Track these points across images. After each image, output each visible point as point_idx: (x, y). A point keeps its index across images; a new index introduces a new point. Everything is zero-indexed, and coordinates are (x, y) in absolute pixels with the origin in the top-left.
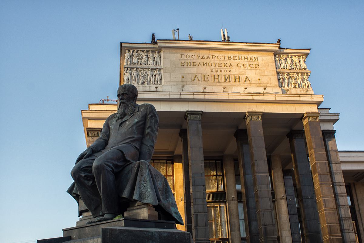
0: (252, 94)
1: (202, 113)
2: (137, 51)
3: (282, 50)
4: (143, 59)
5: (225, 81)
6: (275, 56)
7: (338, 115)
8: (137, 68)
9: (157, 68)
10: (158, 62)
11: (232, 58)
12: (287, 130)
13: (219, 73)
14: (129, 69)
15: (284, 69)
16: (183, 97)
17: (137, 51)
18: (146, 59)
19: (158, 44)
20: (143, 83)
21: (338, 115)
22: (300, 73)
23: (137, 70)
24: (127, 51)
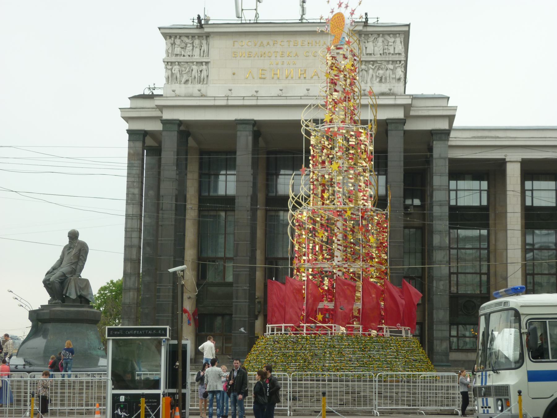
3: (369, 29)
4: (187, 48)
14: (169, 64)
16: (231, 103)
17: (180, 36)
18: (191, 48)
20: (187, 82)
21: (455, 109)
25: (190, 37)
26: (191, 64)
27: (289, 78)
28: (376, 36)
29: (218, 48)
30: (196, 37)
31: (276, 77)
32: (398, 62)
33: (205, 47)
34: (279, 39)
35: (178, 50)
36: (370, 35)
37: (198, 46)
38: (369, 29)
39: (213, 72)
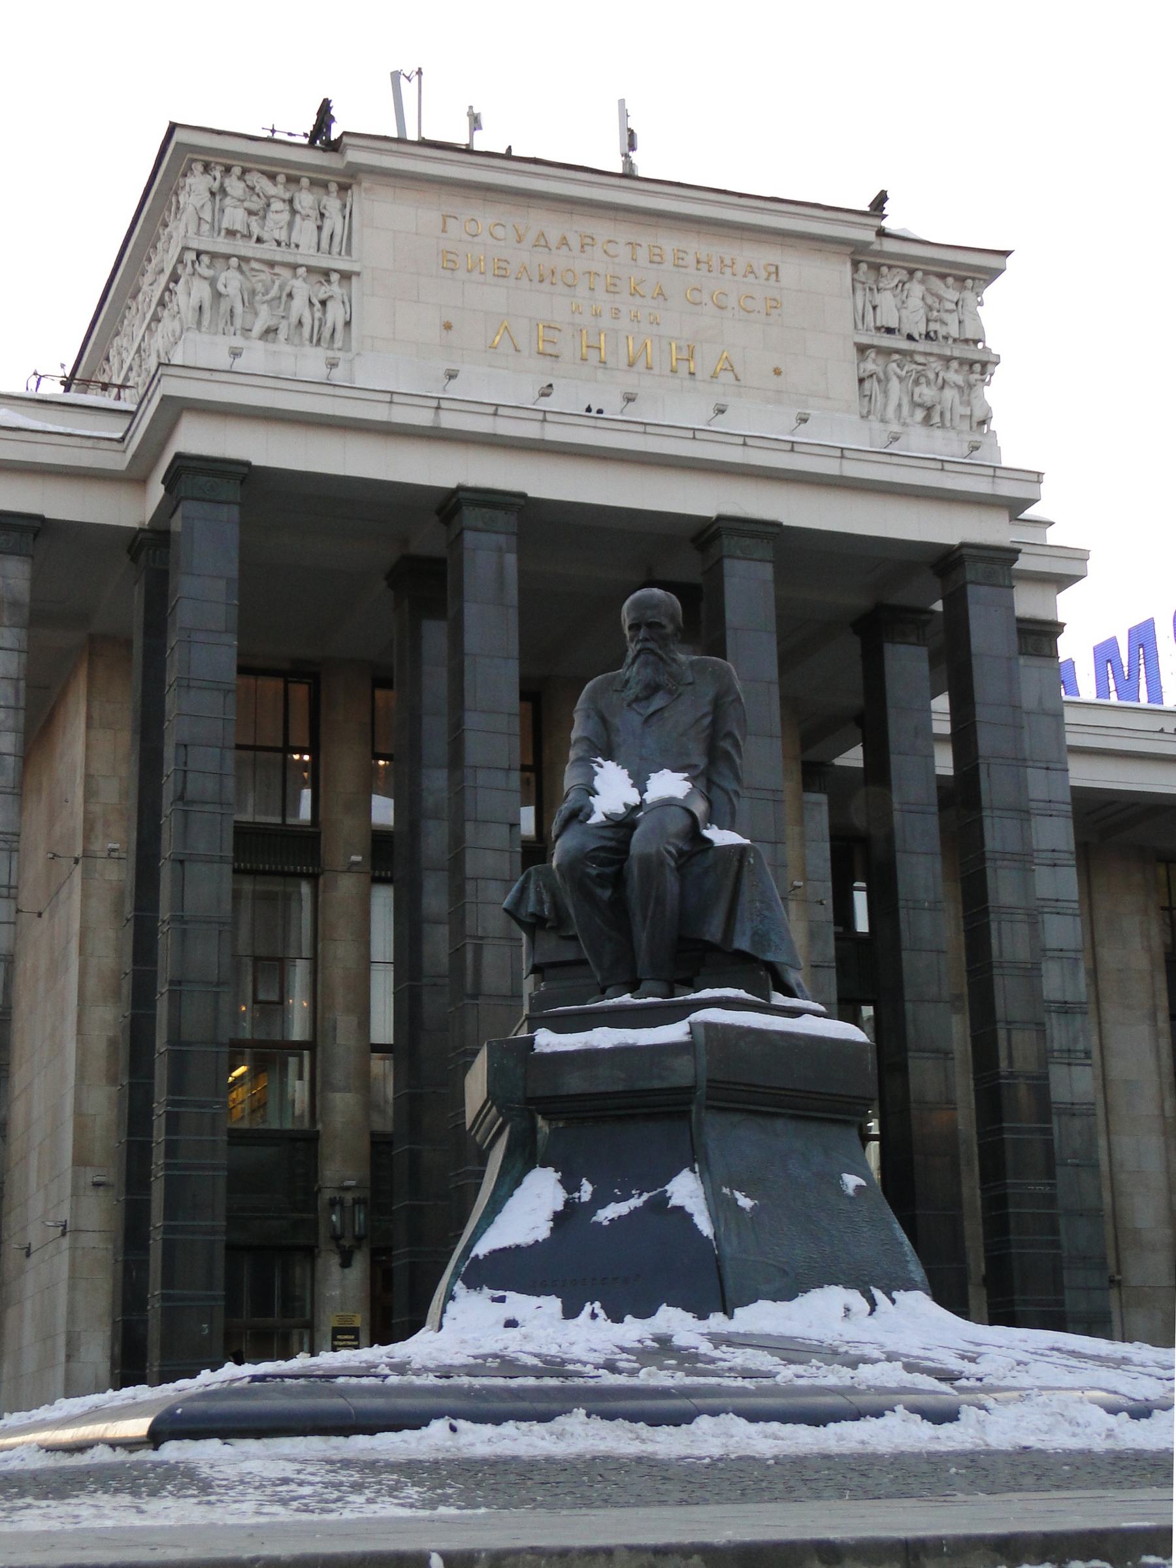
0: (745, 441)
1: (522, 502)
2: (245, 171)
3: (889, 246)
4: (271, 216)
5: (631, 365)
6: (855, 265)
7: (1081, 556)
8: (243, 259)
9: (335, 271)
10: (337, 239)
11: (669, 257)
12: (861, 602)
13: (606, 322)
14: (205, 259)
15: (890, 331)
16: (449, 421)
17: (245, 171)
18: (286, 216)
19: (343, 154)
20: (270, 332)
21: (1081, 556)
22: (956, 358)
23: (239, 268)
24: (198, 168)
25: (281, 179)
26: (286, 273)
27: (640, 366)
28: (904, 275)
29: (386, 225)
30: (305, 182)
31: (593, 356)
32: (977, 367)
33: (334, 222)
34: (601, 229)
35: (235, 217)
36: (884, 270)
37: (314, 214)
38: (889, 246)
39: (371, 310)
